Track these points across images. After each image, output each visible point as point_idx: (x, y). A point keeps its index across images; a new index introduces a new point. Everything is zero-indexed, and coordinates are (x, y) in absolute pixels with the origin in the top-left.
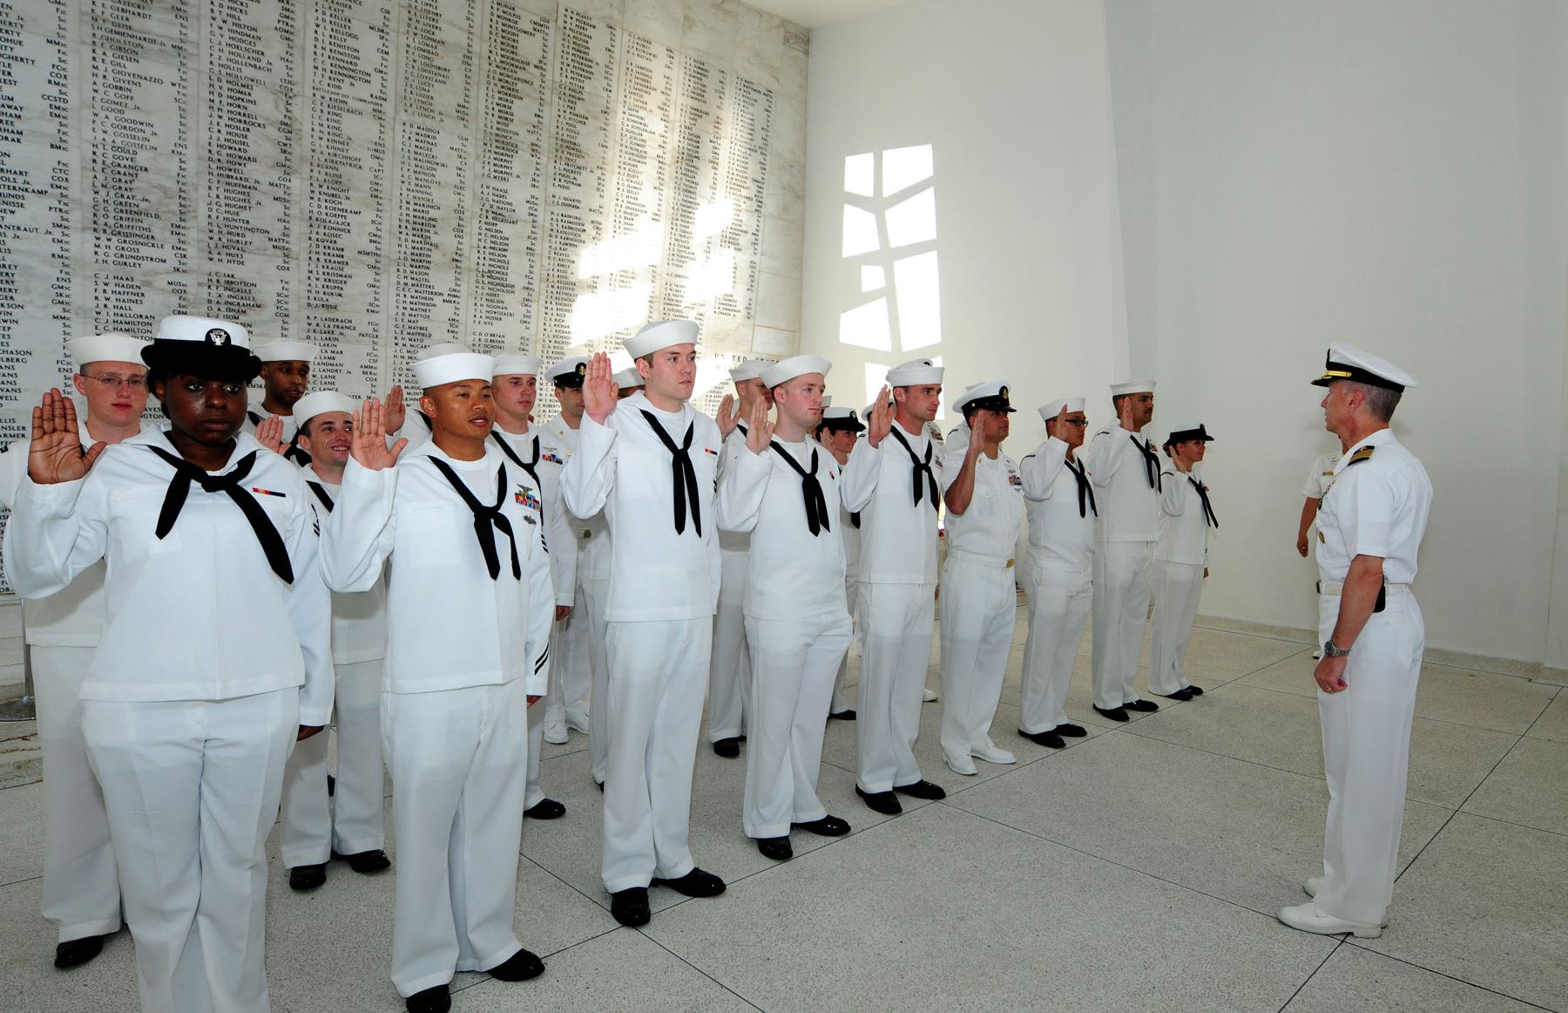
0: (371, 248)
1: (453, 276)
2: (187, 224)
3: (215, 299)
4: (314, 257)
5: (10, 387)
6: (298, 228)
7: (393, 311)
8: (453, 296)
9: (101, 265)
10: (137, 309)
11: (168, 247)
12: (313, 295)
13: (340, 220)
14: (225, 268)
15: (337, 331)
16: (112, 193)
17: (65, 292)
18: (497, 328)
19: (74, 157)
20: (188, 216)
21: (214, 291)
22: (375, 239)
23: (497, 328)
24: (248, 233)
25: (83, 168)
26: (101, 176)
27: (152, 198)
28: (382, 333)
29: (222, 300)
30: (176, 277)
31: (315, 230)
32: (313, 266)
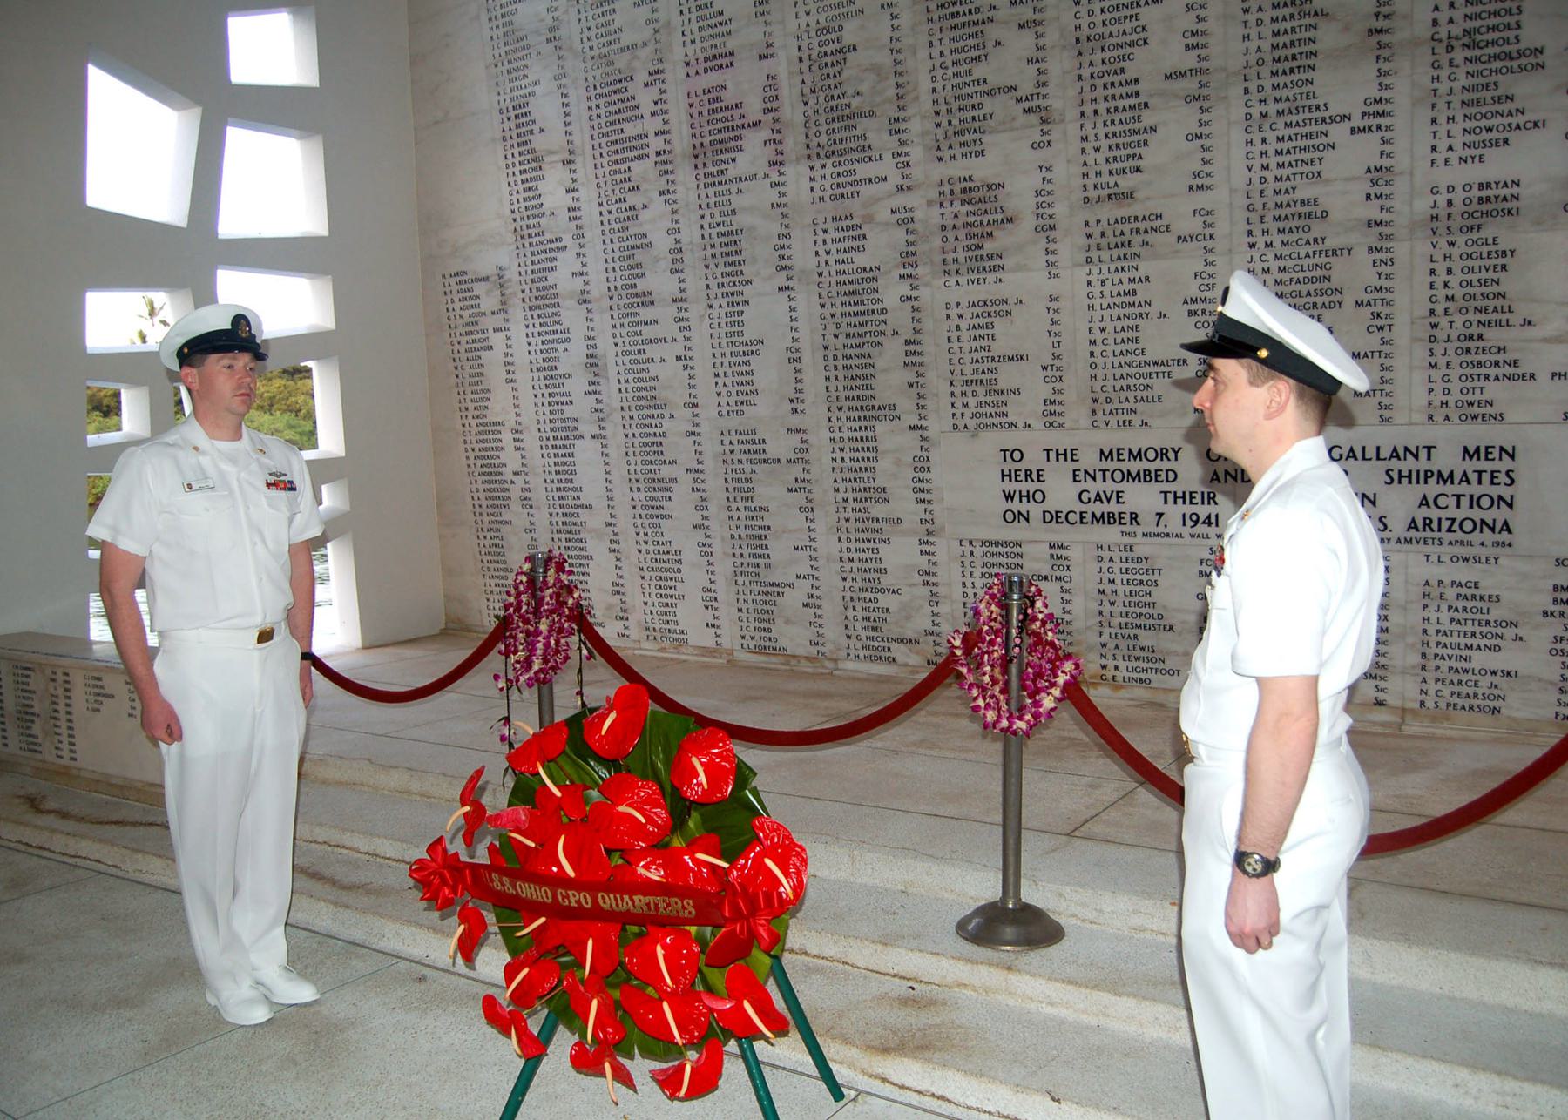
0: (1190, 60)
1: (1370, 69)
2: (910, 112)
3: (949, 222)
4: (1089, 109)
5: (748, 388)
6: (1060, 65)
7: (1240, 176)
8: (1377, 112)
9: (818, 205)
10: (861, 260)
11: (887, 156)
12: (1090, 183)
13: (1128, 26)
14: (958, 169)
15: (1137, 239)
16: (822, 96)
17: (786, 252)
18: (1497, 165)
19: (782, 66)
20: (909, 97)
21: (948, 210)
22: (1195, 41)
23: (1497, 165)
24: (989, 105)
25: (791, 73)
26: (808, 79)
27: (863, 88)
28: (1221, 229)
29: (959, 223)
30: (900, 201)
31: (1086, 60)
32: (1088, 125)
